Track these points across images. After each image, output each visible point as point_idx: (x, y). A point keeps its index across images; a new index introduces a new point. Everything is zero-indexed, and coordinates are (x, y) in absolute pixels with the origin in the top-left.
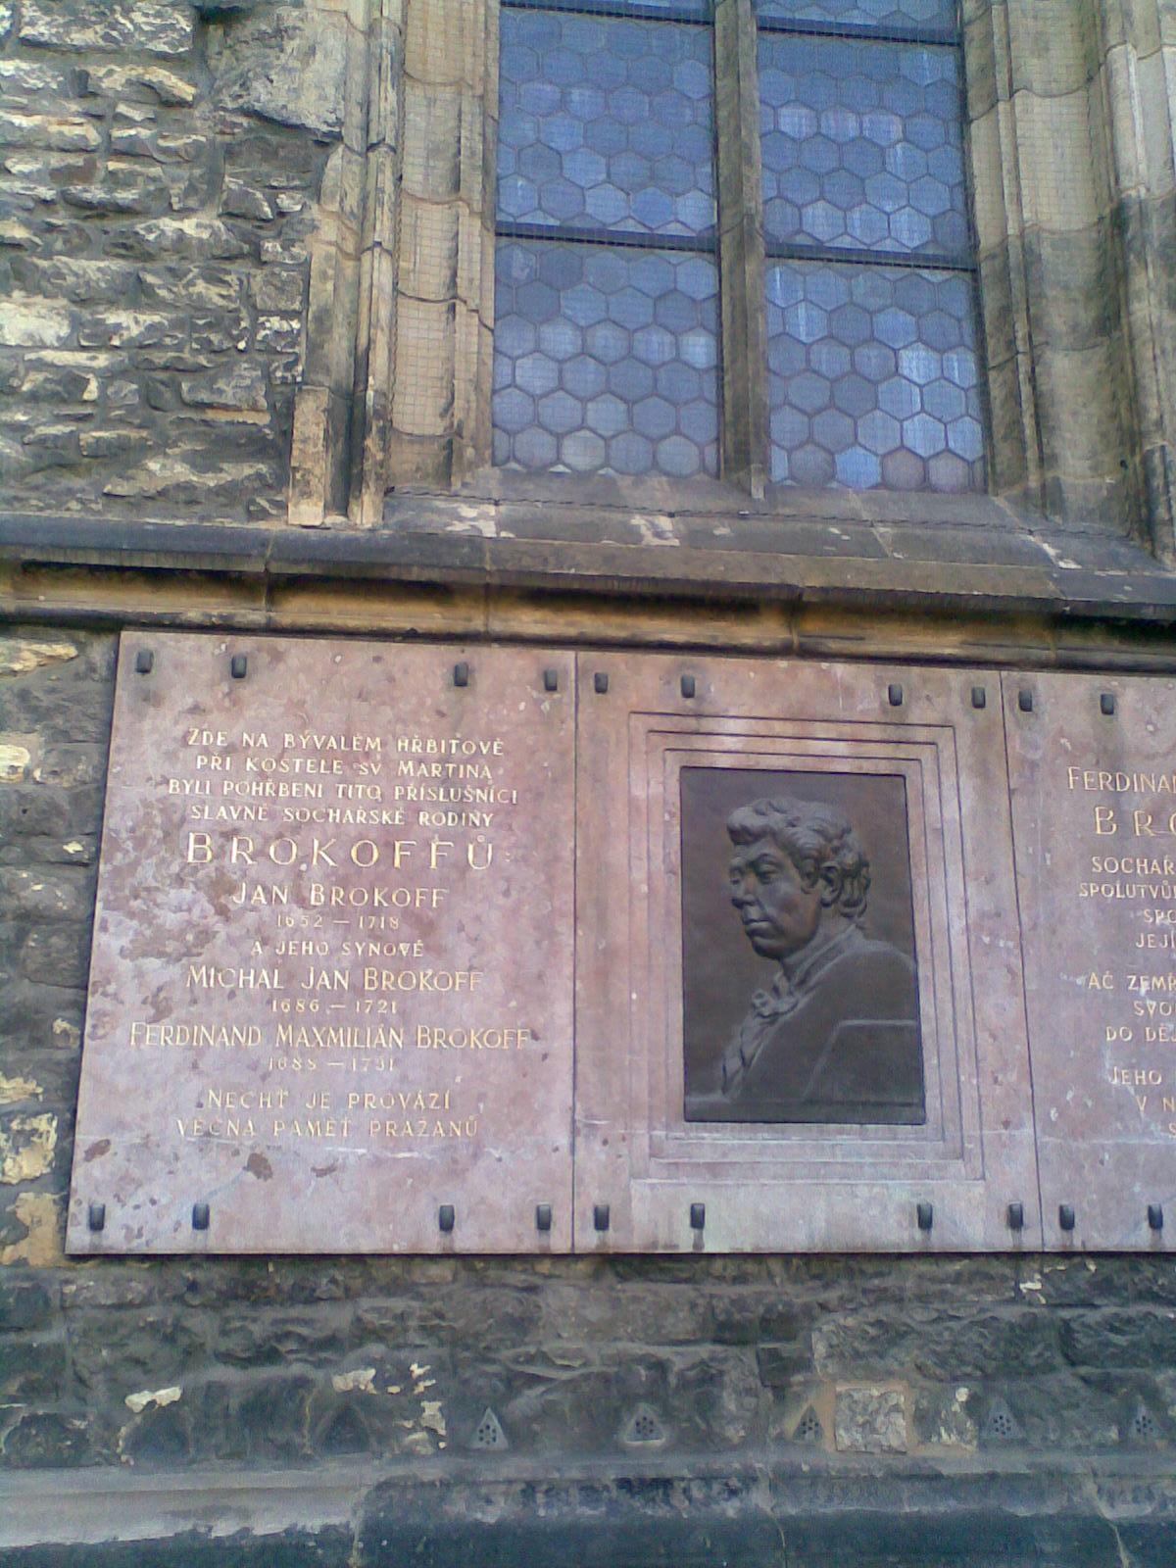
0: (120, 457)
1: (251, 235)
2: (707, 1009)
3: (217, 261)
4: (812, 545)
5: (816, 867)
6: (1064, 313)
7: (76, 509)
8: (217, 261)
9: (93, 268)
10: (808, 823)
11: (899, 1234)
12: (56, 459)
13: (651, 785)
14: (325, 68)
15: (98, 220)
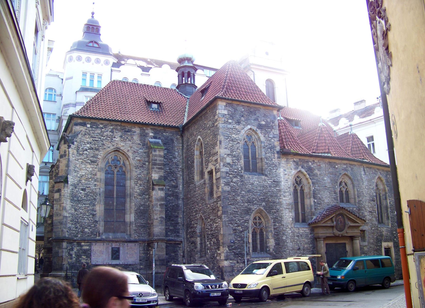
0: (91, 236)
1: (95, 226)
2: (112, 256)
3: (94, 227)
4: (117, 238)
5: (116, 251)
6: (129, 225)
7: (89, 238)
8: (94, 227)
9: (89, 227)
10: (116, 249)
11: (118, 264)
12: (88, 236)
13: (110, 248)
14: (98, 218)
15: (89, 226)
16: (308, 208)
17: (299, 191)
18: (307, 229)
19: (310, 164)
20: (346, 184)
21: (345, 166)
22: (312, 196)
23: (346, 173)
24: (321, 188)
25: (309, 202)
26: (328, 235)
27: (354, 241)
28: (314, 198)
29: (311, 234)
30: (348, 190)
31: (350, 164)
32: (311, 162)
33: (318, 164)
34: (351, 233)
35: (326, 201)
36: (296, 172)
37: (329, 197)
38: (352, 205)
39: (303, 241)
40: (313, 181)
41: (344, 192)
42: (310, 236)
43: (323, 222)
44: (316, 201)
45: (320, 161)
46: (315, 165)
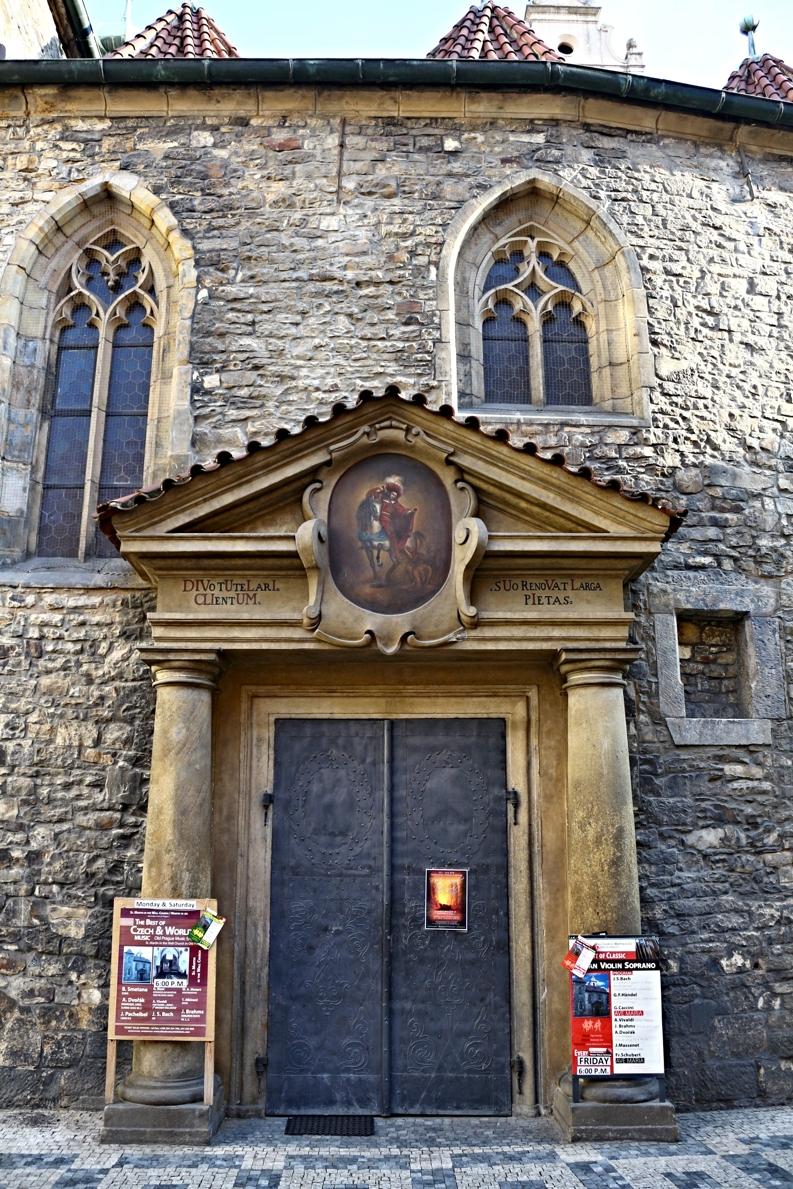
16: (158, 445)
17: (104, 331)
18: (96, 599)
19: (205, 138)
20: (559, 268)
21: (540, 139)
22: (184, 350)
23: (546, 180)
24: (274, 290)
25: (169, 394)
26: (247, 640)
27: (576, 701)
28: (200, 360)
29: (126, 635)
30: (577, 308)
31: (587, 127)
32: (215, 129)
33: (280, 136)
34: (517, 623)
35: (309, 377)
36: (68, 197)
37: (346, 352)
38: (614, 412)
39: (49, 691)
40: (205, 245)
41: (535, 326)
42: (117, 655)
43: (184, 519)
44: (211, 381)
45: (295, 120)
46: (251, 145)
